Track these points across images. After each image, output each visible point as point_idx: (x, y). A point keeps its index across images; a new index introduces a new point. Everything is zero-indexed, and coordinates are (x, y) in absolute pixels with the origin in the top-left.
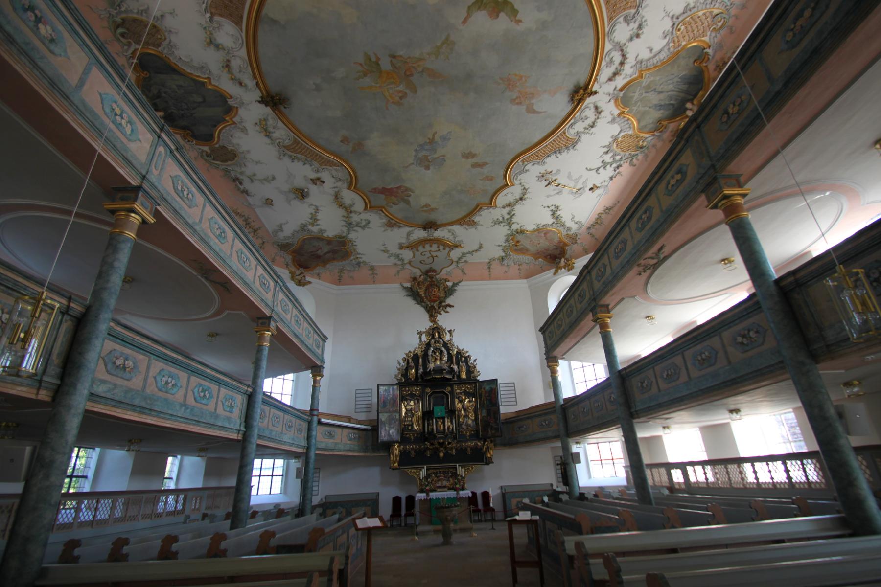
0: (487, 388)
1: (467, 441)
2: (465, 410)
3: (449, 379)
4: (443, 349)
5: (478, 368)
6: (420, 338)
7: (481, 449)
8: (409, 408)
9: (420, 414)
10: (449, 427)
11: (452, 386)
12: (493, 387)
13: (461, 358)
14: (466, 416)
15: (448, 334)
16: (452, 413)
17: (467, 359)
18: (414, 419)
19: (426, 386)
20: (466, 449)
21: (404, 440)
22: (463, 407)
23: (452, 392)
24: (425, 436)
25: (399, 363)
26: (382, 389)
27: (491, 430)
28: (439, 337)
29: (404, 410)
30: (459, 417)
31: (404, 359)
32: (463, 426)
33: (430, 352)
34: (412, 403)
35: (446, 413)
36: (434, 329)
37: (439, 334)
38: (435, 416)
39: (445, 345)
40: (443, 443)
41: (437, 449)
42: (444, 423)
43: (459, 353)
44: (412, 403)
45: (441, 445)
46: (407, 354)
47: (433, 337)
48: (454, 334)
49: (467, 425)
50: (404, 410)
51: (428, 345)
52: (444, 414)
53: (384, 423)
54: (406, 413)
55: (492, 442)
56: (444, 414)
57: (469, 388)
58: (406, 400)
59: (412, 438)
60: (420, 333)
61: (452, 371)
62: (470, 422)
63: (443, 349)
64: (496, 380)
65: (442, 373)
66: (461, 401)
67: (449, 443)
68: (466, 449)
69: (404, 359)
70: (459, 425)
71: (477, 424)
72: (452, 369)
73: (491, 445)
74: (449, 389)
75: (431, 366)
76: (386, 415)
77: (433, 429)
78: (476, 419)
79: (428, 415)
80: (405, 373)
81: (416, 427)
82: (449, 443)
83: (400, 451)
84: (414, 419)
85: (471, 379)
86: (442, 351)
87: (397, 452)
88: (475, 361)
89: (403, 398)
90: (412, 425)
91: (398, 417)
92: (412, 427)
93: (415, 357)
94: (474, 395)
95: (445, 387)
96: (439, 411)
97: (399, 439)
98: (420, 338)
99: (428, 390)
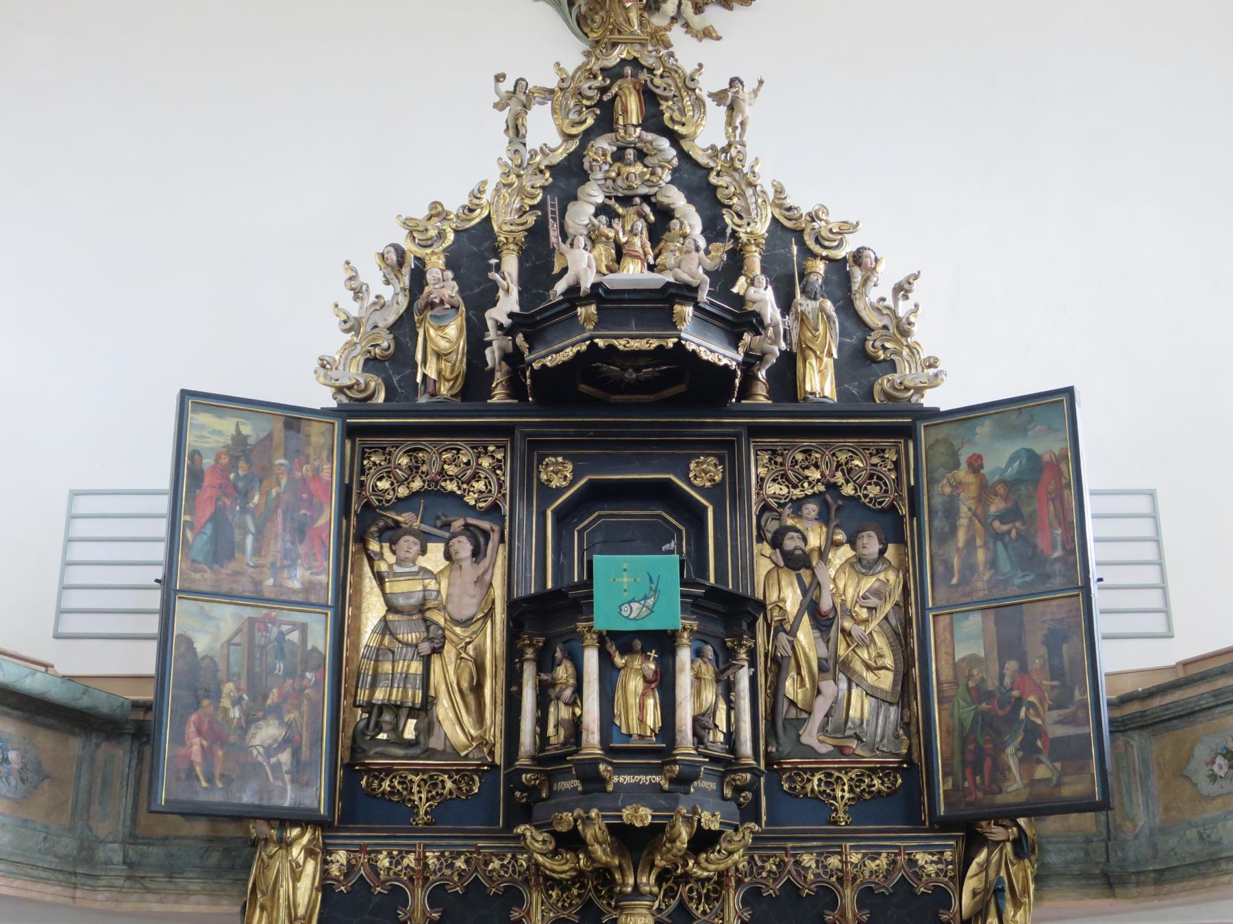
0: (999, 457)
1: (833, 841)
2: (822, 622)
3: (711, 385)
4: (676, 198)
5: (925, 337)
6: (516, 131)
7: (942, 897)
8: (406, 588)
9: (493, 639)
10: (701, 724)
11: (728, 450)
12: (1047, 446)
13: (808, 259)
14: (831, 667)
15: (716, 113)
16: (728, 615)
17: (844, 278)
18: (446, 673)
19: (539, 447)
20: (827, 897)
21: (359, 798)
22: (812, 607)
23: (730, 491)
24: (514, 790)
25: (358, 293)
26: (199, 419)
27: (1029, 754)
28: (653, 121)
29: (373, 611)
30: (778, 666)
31: (396, 260)
32: (810, 736)
33: (581, 214)
34: (434, 558)
35: (692, 605)
36: (613, 74)
37: (650, 98)
38: (605, 617)
39: (696, 180)
40: (656, 833)
41: (604, 875)
42: (664, 684)
43: (789, 232)
44: (434, 558)
45: (635, 843)
46: (413, 229)
47: (606, 120)
48: (749, 110)
49: (836, 724)
50: (373, 611)
51: (569, 174)
52: (668, 613)
53: (201, 685)
54: (385, 628)
55: (1021, 847)
56: (668, 613)
57: (856, 469)
58: (392, 533)
59: (422, 800)
60: (519, 99)
61: (738, 321)
62: (859, 706)
63: (676, 198)
64: (1069, 392)
65: (669, 322)
66: (796, 562)
67: (704, 841)
68: (827, 897)
69: (396, 260)
70: (776, 720)
71: (915, 727)
72: (740, 300)
73: (1022, 873)
74: (704, 472)
75: (582, 265)
76: (228, 618)
77: (576, 726)
78: (905, 690)
79: (545, 621)
80: (395, 359)
81: (454, 726)
82: (704, 841)
83: (326, 887)
84: (446, 673)
85: (881, 417)
86: (665, 214)
87: (305, 891)
88: (902, 290)
89: (366, 523)
90: (424, 709)
91: (319, 636)
92: (428, 727)
93: (473, 250)
94: (892, 526)
95: (682, 448)
96: (635, 587)
97: (316, 797)
98: (516, 131)
99: (559, 474)
